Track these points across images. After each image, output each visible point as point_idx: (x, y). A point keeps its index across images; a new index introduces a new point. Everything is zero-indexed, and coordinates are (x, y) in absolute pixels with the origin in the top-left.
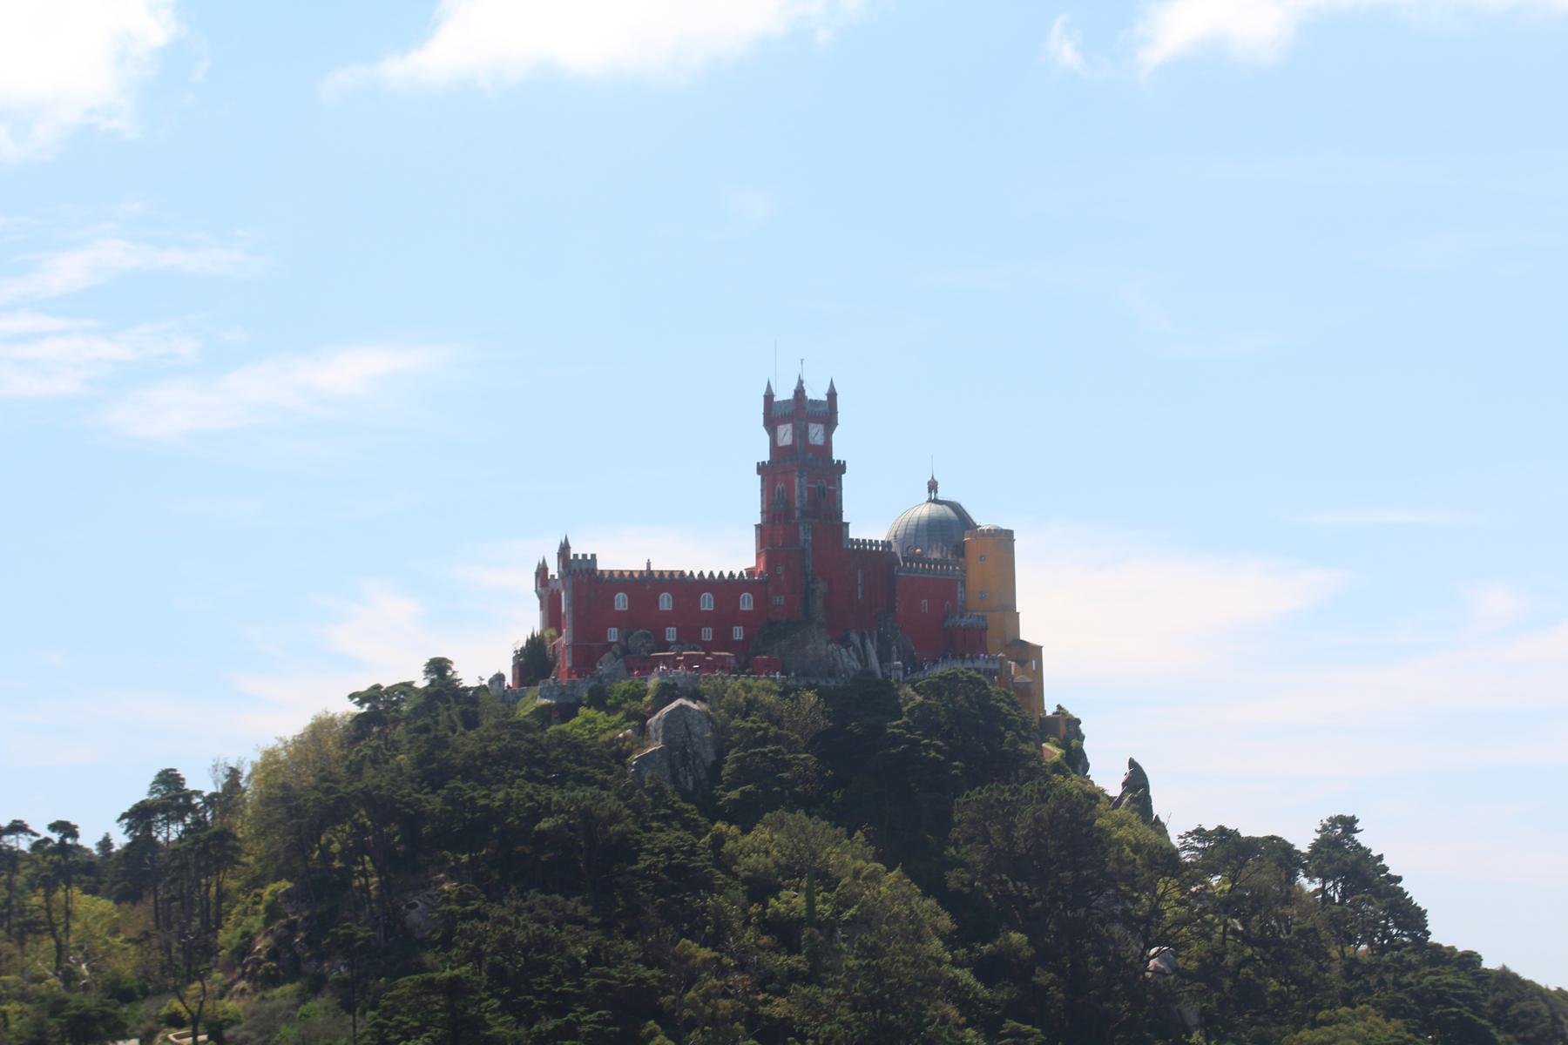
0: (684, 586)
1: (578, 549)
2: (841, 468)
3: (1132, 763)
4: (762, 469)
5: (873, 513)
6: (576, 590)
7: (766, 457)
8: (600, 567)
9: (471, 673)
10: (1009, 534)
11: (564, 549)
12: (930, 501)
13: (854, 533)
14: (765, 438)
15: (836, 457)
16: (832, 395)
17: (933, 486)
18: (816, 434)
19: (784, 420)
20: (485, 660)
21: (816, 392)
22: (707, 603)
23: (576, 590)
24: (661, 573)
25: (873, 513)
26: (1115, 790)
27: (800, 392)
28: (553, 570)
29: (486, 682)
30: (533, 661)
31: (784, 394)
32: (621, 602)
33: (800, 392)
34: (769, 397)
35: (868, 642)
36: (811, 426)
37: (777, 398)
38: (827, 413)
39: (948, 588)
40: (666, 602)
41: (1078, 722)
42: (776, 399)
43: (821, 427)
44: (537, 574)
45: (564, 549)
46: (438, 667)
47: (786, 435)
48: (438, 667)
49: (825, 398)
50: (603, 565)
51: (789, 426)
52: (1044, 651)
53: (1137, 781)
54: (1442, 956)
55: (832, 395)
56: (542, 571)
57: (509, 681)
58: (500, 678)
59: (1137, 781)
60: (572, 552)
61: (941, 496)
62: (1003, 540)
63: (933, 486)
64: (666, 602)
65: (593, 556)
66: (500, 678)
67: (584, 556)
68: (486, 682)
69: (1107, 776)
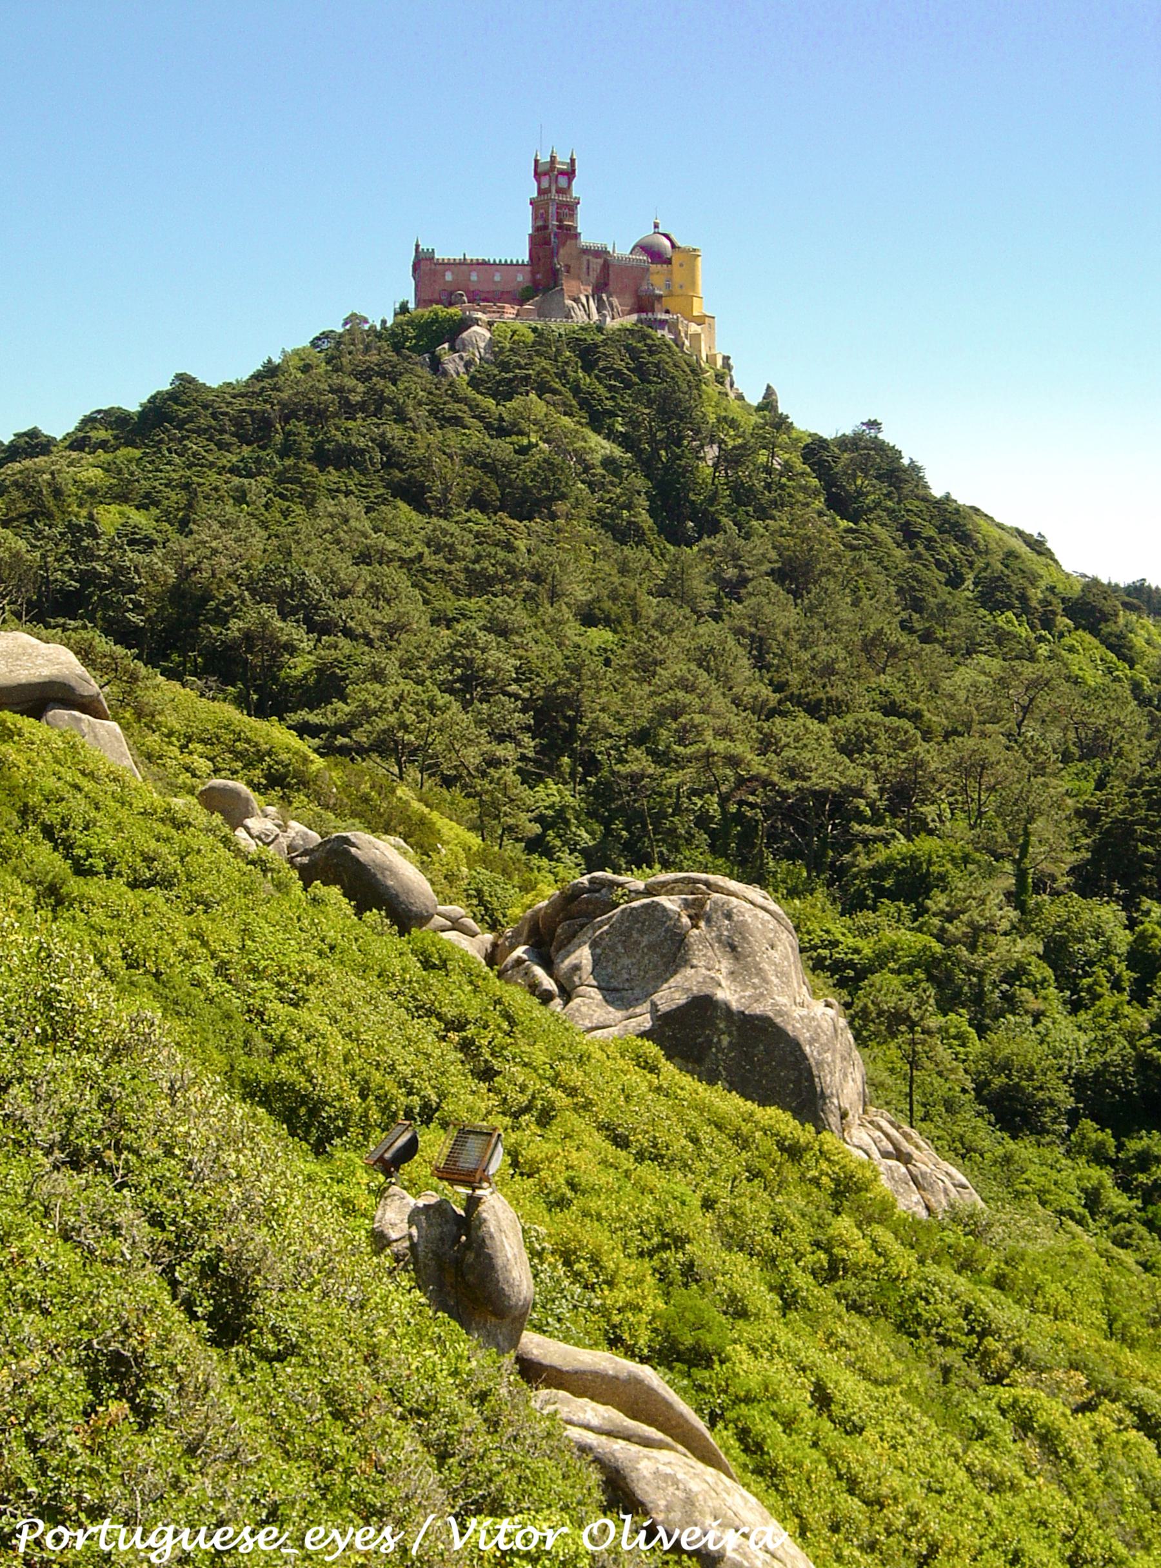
3: (769, 387)
11: (417, 246)
16: (573, 160)
17: (656, 226)
19: (545, 174)
21: (563, 159)
27: (553, 158)
31: (545, 159)
33: (553, 158)
34: (536, 161)
38: (570, 174)
39: (651, 278)
45: (417, 246)
55: (573, 160)
58: (384, 322)
62: (692, 255)
63: (656, 226)
66: (384, 322)
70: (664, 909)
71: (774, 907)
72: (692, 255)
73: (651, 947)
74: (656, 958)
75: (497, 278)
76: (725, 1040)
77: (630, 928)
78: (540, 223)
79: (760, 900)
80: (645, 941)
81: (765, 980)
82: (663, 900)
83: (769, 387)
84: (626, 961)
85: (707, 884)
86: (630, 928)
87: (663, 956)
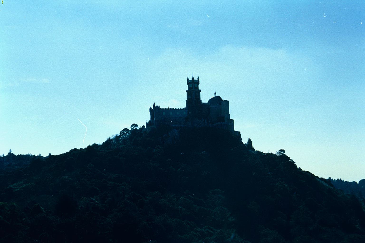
1: (156, 105)
2: (200, 91)
3: (249, 139)
4: (187, 91)
5: (205, 97)
6: (156, 111)
7: (187, 89)
8: (160, 108)
10: (228, 102)
12: (215, 96)
13: (202, 102)
14: (187, 86)
15: (199, 89)
17: (215, 93)
18: (196, 85)
21: (196, 78)
23: (156, 111)
24: (170, 109)
25: (205, 97)
27: (193, 78)
28: (152, 108)
29: (141, 127)
31: (190, 79)
32: (164, 113)
33: (193, 78)
34: (188, 79)
35: (205, 119)
36: (195, 84)
37: (189, 80)
38: (198, 82)
41: (240, 132)
42: (189, 80)
43: (197, 84)
44: (150, 109)
45: (154, 105)
47: (191, 85)
49: (197, 79)
50: (160, 108)
51: (191, 84)
52: (234, 120)
53: (250, 141)
55: (198, 79)
56: (151, 108)
59: (250, 141)
60: (156, 105)
61: (217, 95)
62: (227, 102)
63: (215, 93)
65: (159, 106)
66: (144, 126)
67: (158, 106)
68: (141, 127)
69: (245, 141)
72: (227, 102)
75: (178, 114)
78: (190, 97)
83: (249, 139)
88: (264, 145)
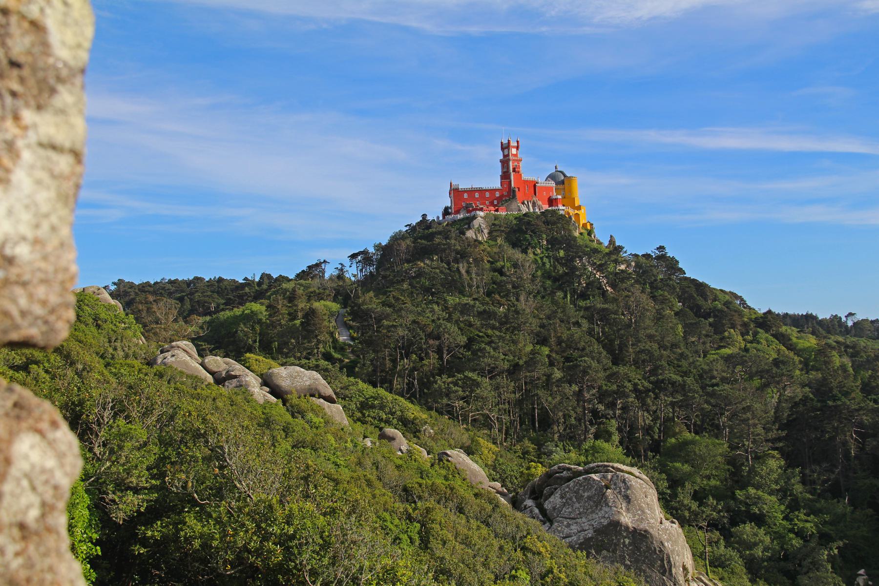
0: (482, 191)
4: (501, 161)
7: (502, 158)
9: (430, 218)
20: (435, 214)
22: (487, 195)
26: (606, 243)
30: (446, 212)
32: (466, 196)
40: (477, 195)
46: (424, 216)
48: (424, 216)
54: (686, 279)
57: (441, 218)
58: (438, 218)
59: (612, 241)
64: (477, 195)
66: (438, 218)
70: (594, 480)
71: (644, 477)
73: (589, 498)
74: (591, 503)
76: (627, 541)
77: (579, 489)
79: (638, 474)
80: (586, 494)
81: (643, 512)
82: (593, 476)
84: (577, 505)
85: (613, 467)
86: (579, 489)
87: (594, 502)
88: (635, 246)
